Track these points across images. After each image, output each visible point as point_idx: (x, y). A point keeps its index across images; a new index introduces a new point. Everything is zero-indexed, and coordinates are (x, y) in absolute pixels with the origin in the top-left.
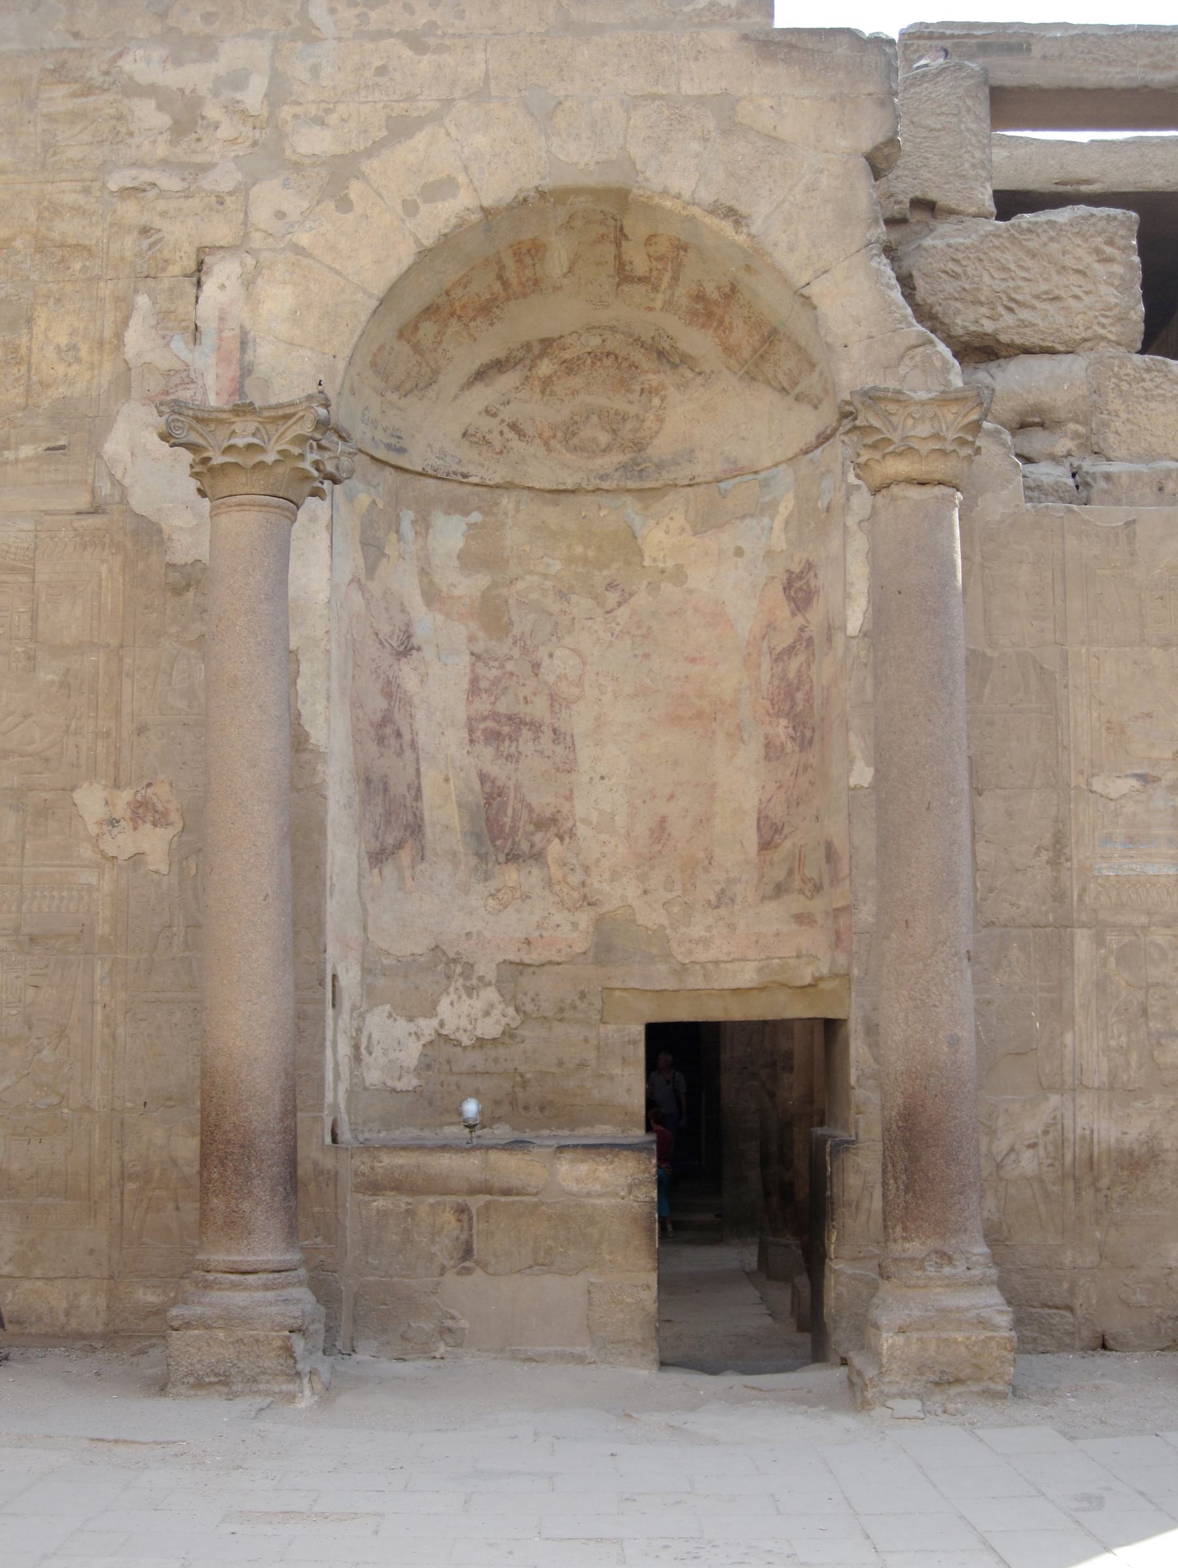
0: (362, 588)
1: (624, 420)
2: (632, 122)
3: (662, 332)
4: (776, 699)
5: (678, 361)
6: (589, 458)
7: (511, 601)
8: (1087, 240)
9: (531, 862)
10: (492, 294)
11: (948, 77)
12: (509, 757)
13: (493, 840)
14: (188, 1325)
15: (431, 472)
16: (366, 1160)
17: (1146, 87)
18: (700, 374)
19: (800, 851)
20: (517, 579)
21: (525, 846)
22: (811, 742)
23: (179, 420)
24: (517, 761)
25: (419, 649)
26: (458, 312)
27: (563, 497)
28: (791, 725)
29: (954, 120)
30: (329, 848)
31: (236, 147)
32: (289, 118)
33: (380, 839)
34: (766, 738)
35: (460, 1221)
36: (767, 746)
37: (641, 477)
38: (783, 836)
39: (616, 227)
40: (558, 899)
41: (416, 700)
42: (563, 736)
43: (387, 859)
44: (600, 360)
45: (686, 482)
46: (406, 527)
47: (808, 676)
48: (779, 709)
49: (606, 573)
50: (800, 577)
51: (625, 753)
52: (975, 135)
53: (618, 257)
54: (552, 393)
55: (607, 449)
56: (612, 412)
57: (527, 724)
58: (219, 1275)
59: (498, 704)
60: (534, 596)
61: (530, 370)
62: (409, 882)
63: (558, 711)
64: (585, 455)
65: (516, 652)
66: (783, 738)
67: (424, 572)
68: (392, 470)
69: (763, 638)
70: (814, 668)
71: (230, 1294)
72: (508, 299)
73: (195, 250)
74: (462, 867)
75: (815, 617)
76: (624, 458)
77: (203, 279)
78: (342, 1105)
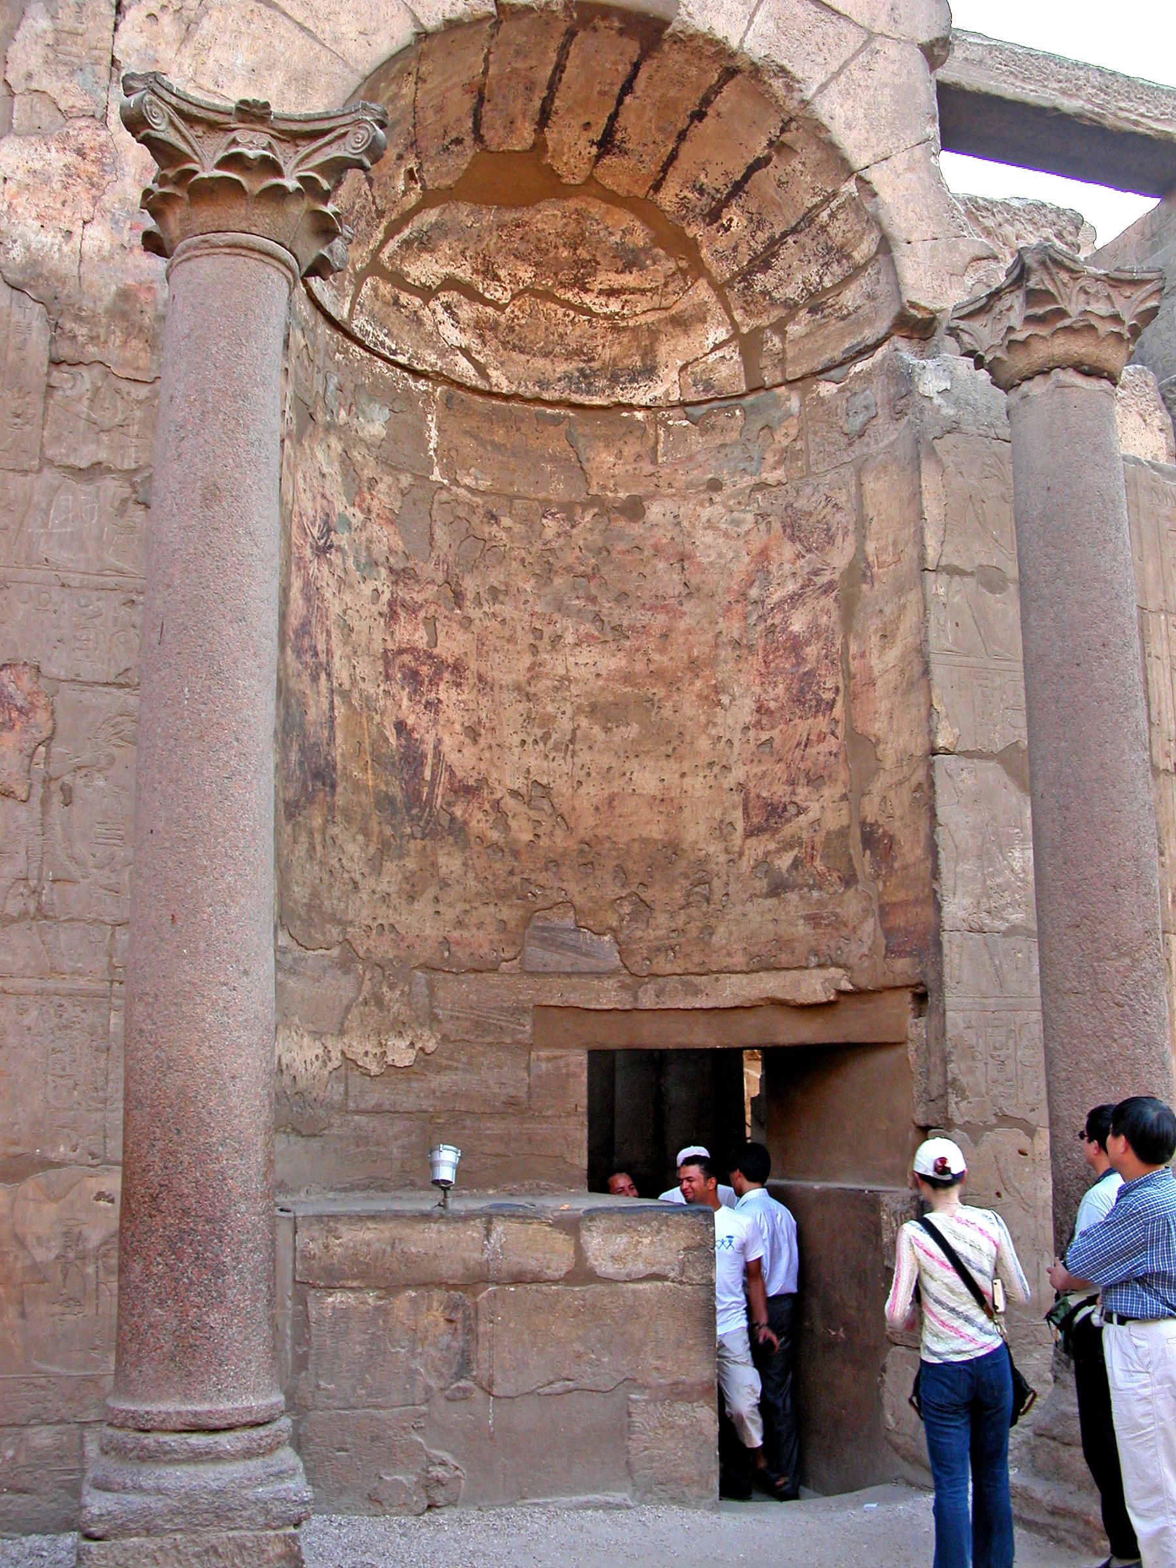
8: (1038, 229)
14: (124, 1530)
16: (316, 1234)
17: (1056, 109)
23: (157, 105)
35: (450, 1321)
57: (449, 666)
58: (168, 1438)
62: (319, 848)
71: (191, 1469)
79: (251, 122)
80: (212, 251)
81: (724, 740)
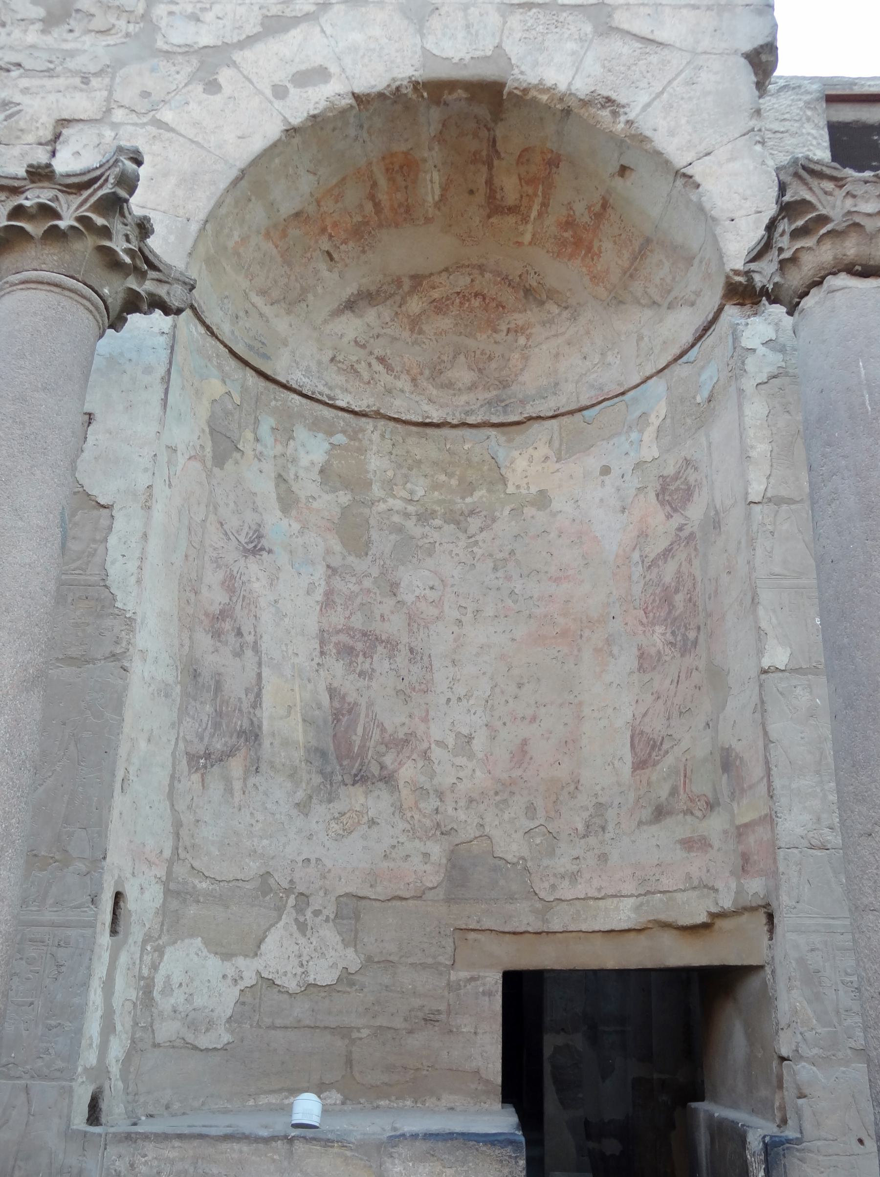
0: (209, 475)
1: (490, 358)
2: (508, 25)
3: (529, 268)
4: (650, 608)
5: (544, 297)
6: (455, 395)
7: (372, 522)
9: (381, 785)
10: (364, 217)
11: (790, 93)
12: (362, 674)
13: (339, 759)
15: (294, 386)
18: (566, 308)
19: (685, 766)
20: (379, 501)
21: (375, 769)
22: (695, 643)
24: (371, 678)
25: (270, 551)
26: (329, 231)
27: (429, 431)
28: (669, 631)
29: (797, 125)
30: (126, 729)
31: (109, 38)
32: (165, 14)
33: (206, 739)
34: (639, 650)
36: (642, 656)
37: (505, 412)
38: (662, 753)
39: (488, 140)
40: (408, 827)
41: (263, 602)
42: (420, 655)
43: (212, 766)
44: (468, 300)
45: (551, 414)
46: (265, 429)
47: (690, 574)
48: (654, 617)
49: (469, 500)
50: (676, 477)
51: (484, 673)
52: (815, 138)
53: (489, 182)
54: (421, 332)
55: (472, 387)
56: (478, 352)
57: (383, 642)
59: (352, 619)
60: (396, 518)
61: (400, 307)
62: (238, 794)
63: (415, 630)
64: (452, 392)
65: (375, 572)
66: (660, 645)
67: (281, 479)
68: (253, 373)
69: (634, 549)
70: (696, 563)
72: (380, 226)
73: (52, 121)
74: (304, 785)
75: (695, 512)
76: (488, 395)
77: (58, 147)
78: (115, 1069)
79: (40, 181)
80: (11, 289)
81: (615, 685)
